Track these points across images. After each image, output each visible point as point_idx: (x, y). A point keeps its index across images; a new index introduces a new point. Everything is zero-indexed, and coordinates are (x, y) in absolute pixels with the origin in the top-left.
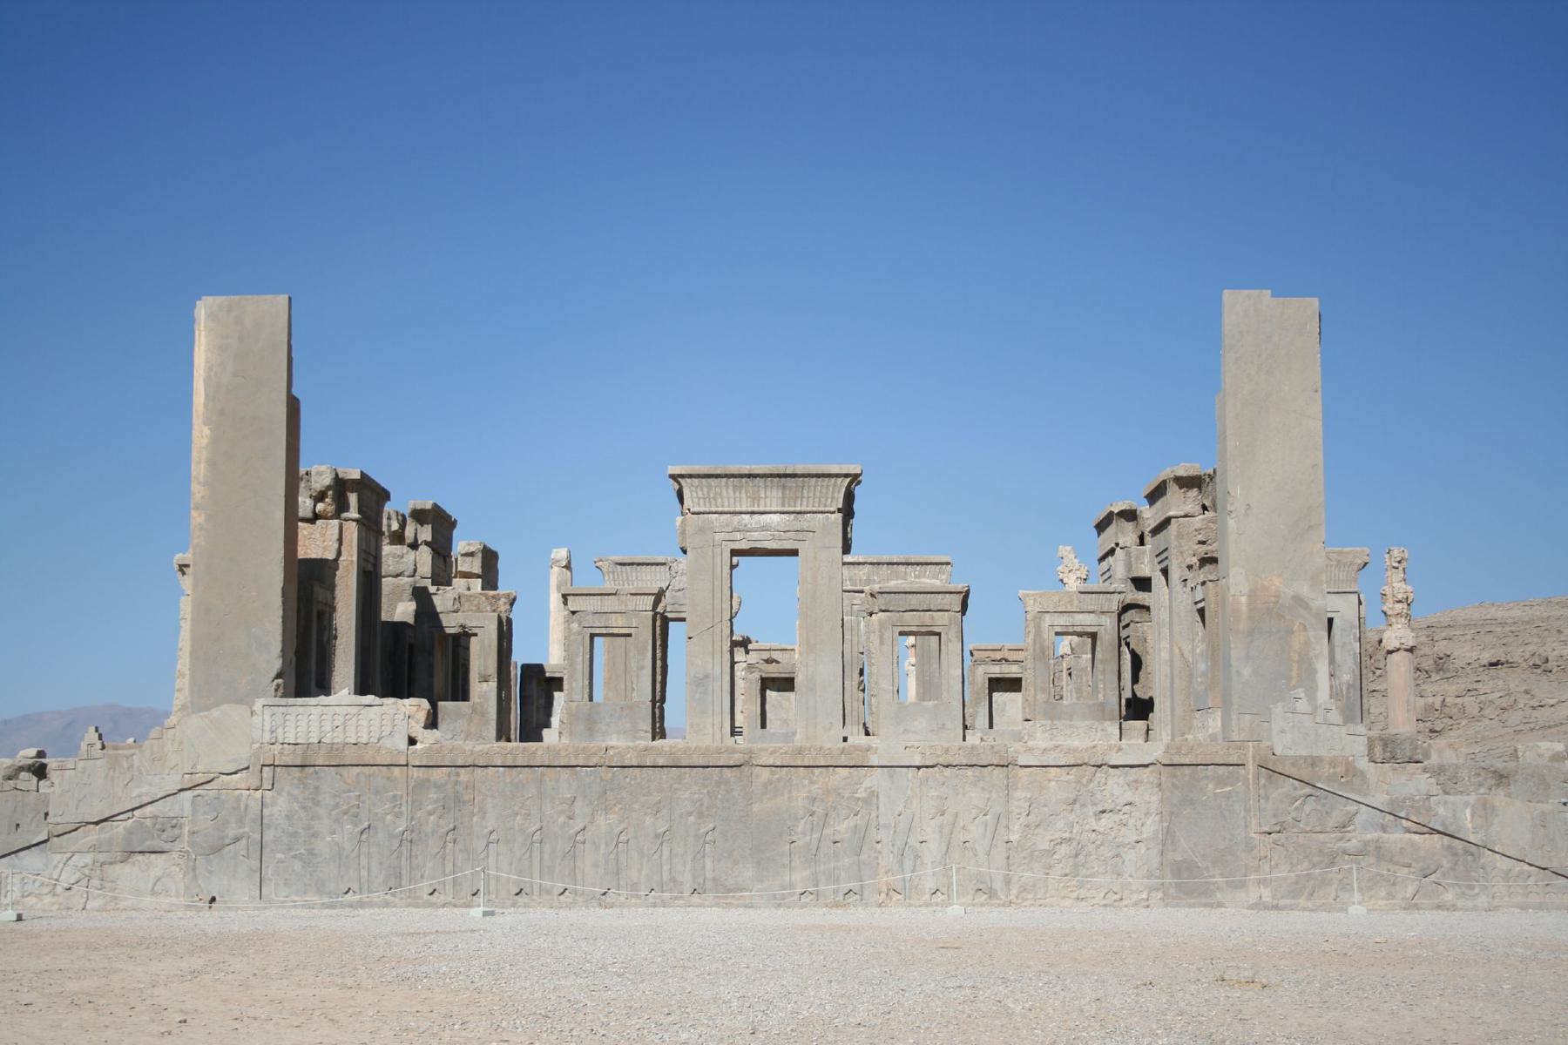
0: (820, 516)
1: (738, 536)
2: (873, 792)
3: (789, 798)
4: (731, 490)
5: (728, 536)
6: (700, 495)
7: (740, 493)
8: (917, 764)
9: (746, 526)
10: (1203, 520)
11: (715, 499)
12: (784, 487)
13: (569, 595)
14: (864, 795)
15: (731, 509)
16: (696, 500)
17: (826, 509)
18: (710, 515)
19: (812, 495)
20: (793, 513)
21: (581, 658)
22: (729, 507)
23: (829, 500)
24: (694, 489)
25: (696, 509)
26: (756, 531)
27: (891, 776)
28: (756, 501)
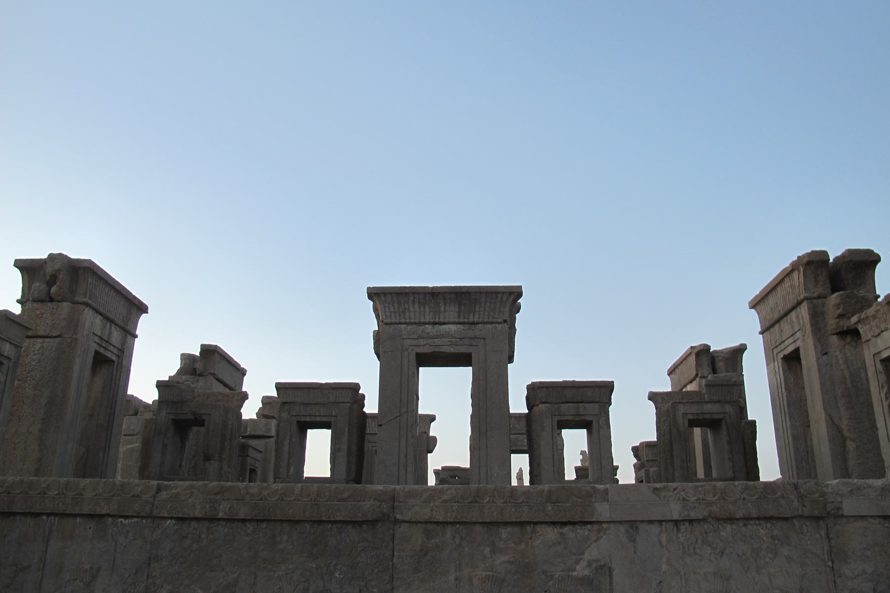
0: (490, 326)
1: (422, 342)
2: (602, 567)
3: (456, 579)
4: (417, 305)
5: (413, 342)
6: (392, 310)
7: (424, 308)
8: (676, 517)
9: (428, 333)
10: (841, 295)
11: (404, 313)
12: (460, 305)
13: (281, 388)
14: (586, 572)
15: (417, 321)
16: (388, 314)
17: (495, 320)
18: (399, 326)
19: (482, 309)
20: (467, 323)
21: (288, 442)
22: (415, 319)
23: (497, 314)
24: (386, 305)
25: (388, 321)
26: (437, 338)
27: (632, 540)
28: (437, 315)
